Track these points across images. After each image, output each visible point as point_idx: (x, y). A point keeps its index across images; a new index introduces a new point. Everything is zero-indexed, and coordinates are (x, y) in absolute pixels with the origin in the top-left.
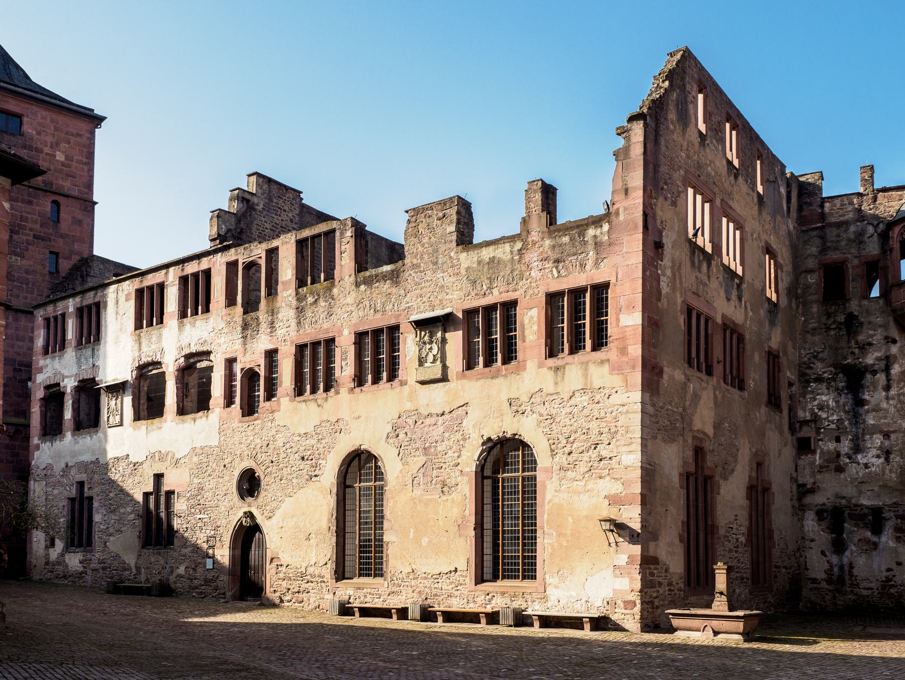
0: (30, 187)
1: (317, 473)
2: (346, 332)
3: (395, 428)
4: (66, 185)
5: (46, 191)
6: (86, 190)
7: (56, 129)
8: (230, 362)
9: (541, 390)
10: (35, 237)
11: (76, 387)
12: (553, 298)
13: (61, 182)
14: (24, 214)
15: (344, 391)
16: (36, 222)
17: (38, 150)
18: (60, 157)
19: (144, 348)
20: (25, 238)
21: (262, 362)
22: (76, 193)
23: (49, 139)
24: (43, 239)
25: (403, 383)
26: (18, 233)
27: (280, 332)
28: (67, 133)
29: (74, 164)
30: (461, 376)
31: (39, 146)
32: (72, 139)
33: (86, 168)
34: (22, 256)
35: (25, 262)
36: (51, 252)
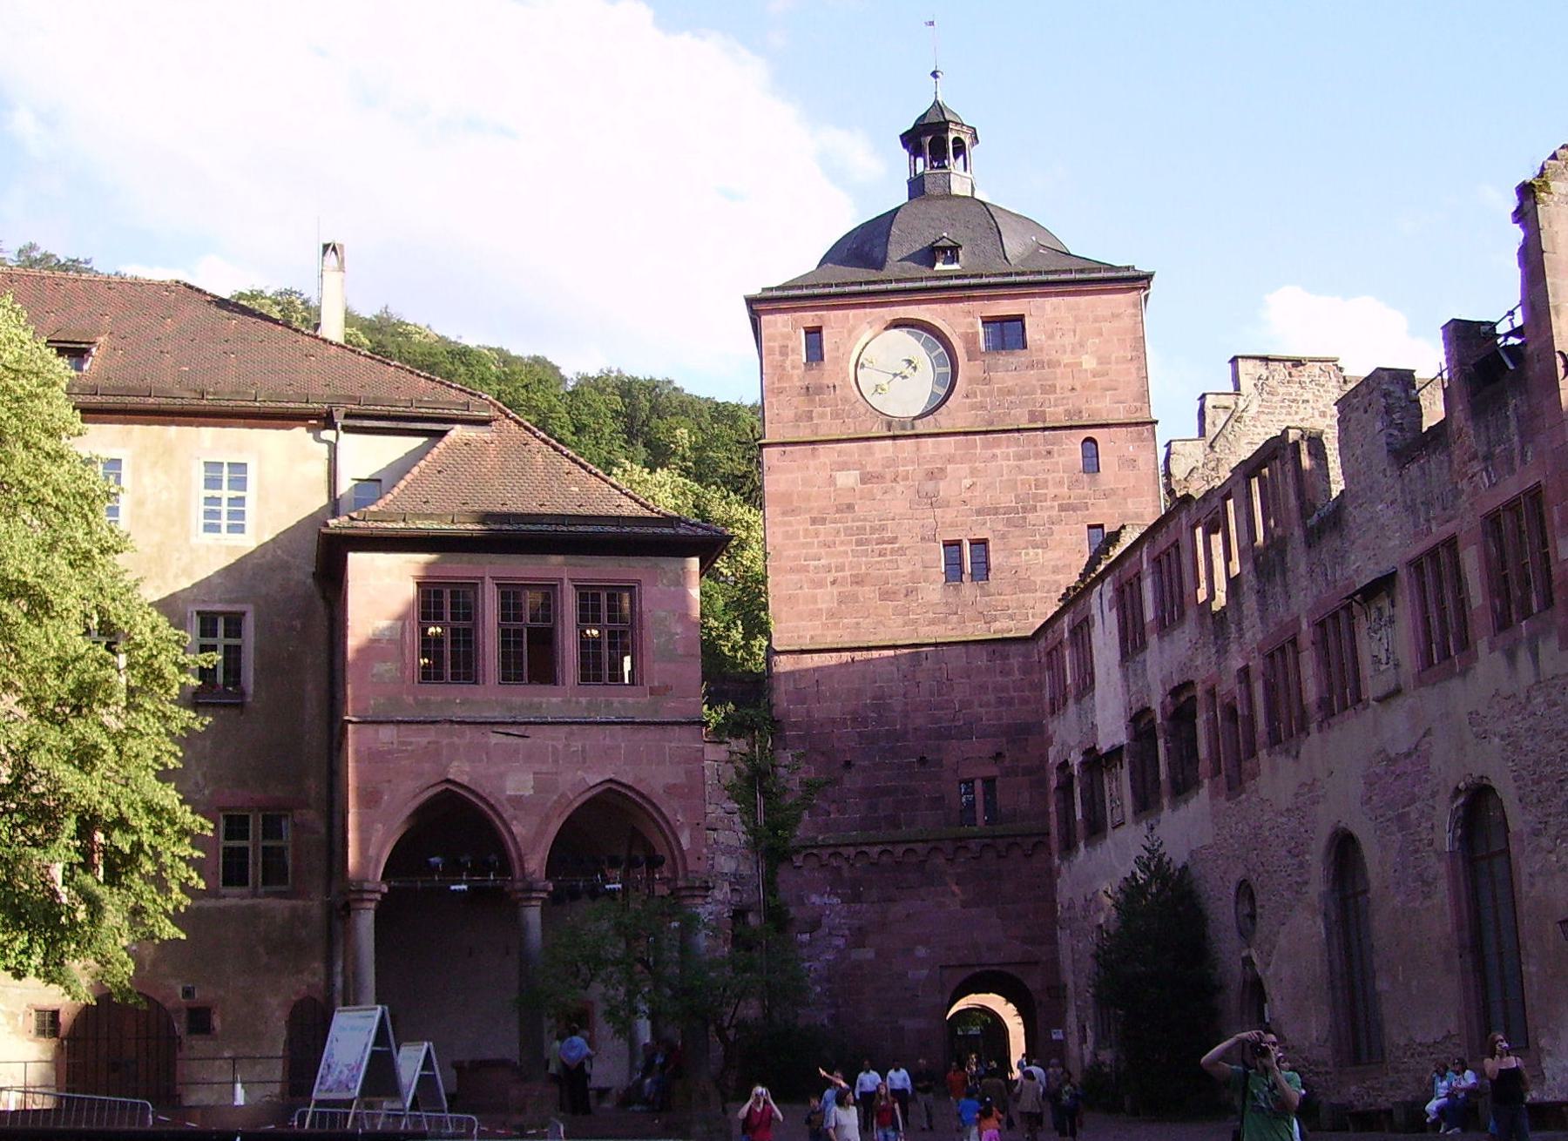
0: (1045, 429)
1: (1306, 877)
2: (1304, 626)
3: (1370, 784)
4: (1106, 407)
5: (1071, 427)
6: (1138, 404)
7: (1077, 319)
8: (1211, 693)
9: (1497, 693)
10: (1062, 508)
11: (1082, 764)
12: (1492, 521)
13: (1094, 405)
14: (1041, 476)
15: (1313, 726)
16: (1061, 483)
17: (1051, 364)
18: (1089, 362)
19: (1133, 689)
20: (1045, 515)
21: (1237, 689)
22: (1121, 417)
23: (1068, 340)
24: (1075, 509)
25: (1367, 706)
26: (1034, 509)
27: (1248, 635)
28: (1096, 320)
29: (1114, 367)
30: (1420, 681)
31: (1054, 356)
32: (1105, 326)
33: (1133, 367)
34: (1044, 546)
35: (1049, 554)
36: (1090, 527)
